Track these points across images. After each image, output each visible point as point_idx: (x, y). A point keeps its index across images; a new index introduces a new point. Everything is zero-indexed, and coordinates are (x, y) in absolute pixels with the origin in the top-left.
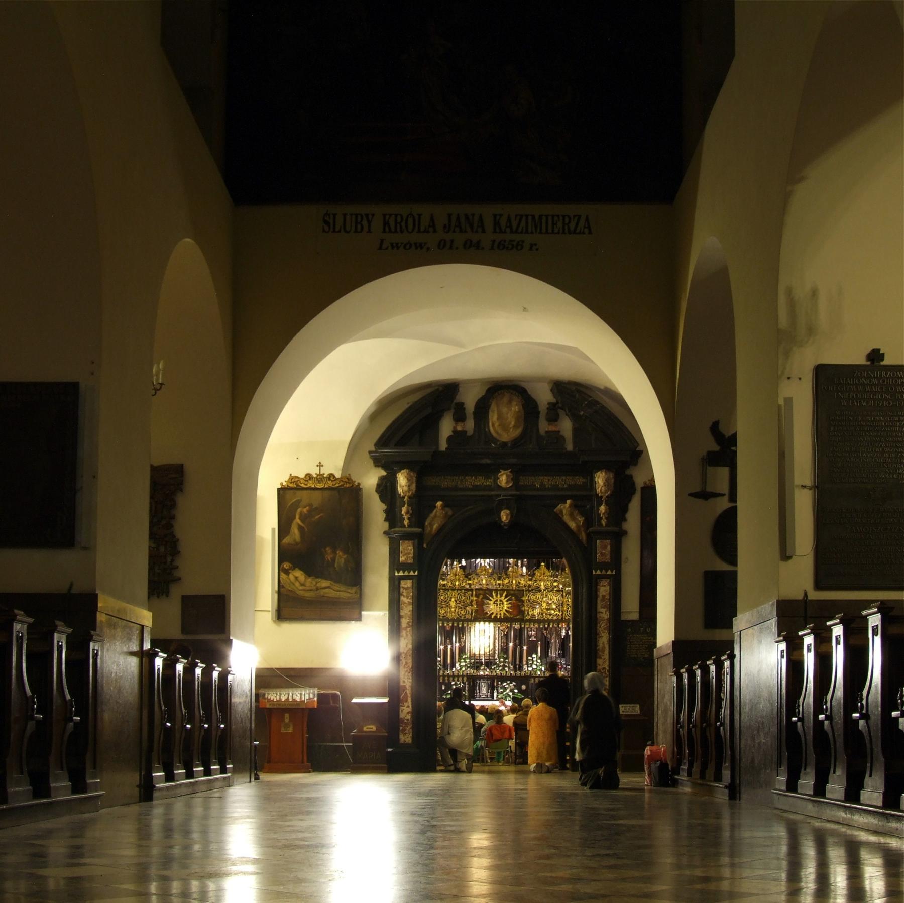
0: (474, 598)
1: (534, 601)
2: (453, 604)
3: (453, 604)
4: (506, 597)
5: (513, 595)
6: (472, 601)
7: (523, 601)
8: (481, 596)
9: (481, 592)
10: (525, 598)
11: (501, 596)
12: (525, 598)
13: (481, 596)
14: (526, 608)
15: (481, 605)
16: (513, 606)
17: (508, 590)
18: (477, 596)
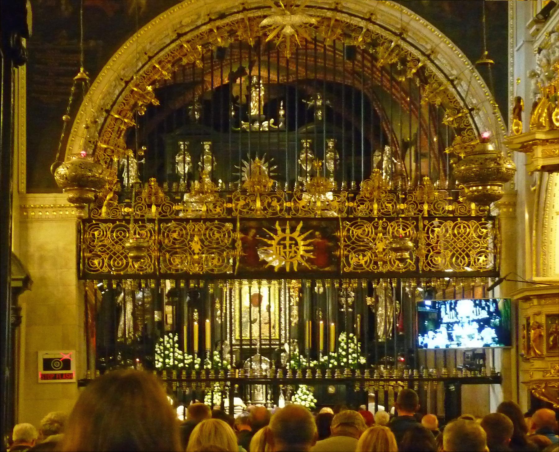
0: (239, 235)
1: (359, 239)
2: (196, 246)
3: (196, 246)
4: (302, 232)
5: (316, 228)
6: (234, 241)
7: (338, 239)
8: (253, 232)
9: (252, 224)
10: (342, 234)
11: (293, 230)
12: (342, 234)
13: (253, 232)
14: (342, 252)
15: (251, 248)
16: (317, 249)
17: (305, 220)
18: (245, 230)
